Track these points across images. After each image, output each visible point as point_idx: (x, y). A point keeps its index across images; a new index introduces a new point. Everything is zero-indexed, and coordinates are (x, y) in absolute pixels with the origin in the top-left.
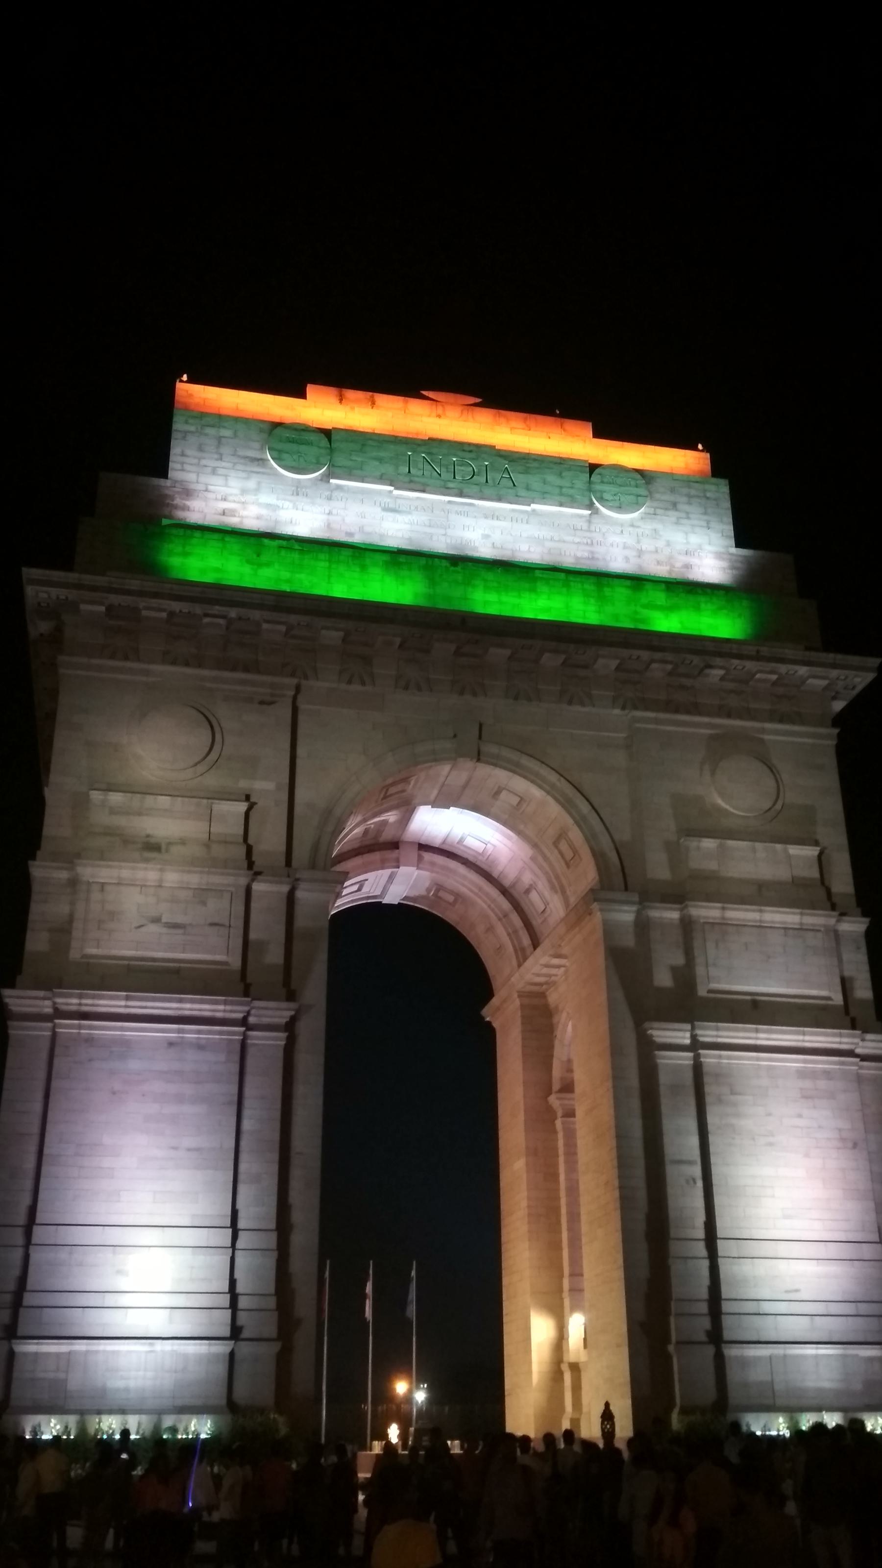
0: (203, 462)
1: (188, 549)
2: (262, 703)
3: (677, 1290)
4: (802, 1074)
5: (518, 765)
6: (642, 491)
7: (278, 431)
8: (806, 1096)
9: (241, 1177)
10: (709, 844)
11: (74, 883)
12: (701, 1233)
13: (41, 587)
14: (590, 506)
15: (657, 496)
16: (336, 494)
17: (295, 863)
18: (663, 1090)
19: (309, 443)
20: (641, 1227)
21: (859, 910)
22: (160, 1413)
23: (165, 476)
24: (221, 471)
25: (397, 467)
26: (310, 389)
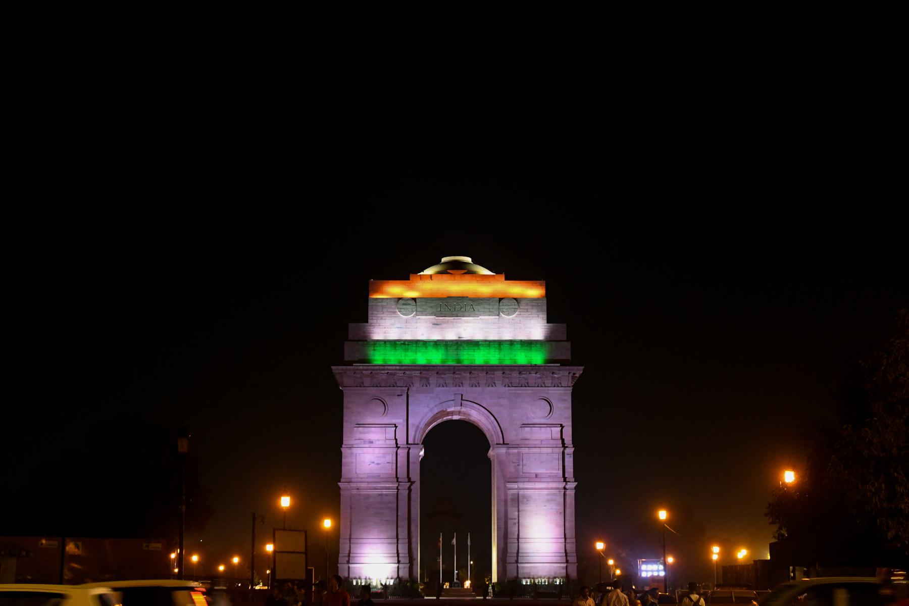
3: (509, 551)
4: (548, 495)
8: (548, 501)
10: (527, 429)
11: (352, 453)
14: (498, 315)
20: (502, 535)
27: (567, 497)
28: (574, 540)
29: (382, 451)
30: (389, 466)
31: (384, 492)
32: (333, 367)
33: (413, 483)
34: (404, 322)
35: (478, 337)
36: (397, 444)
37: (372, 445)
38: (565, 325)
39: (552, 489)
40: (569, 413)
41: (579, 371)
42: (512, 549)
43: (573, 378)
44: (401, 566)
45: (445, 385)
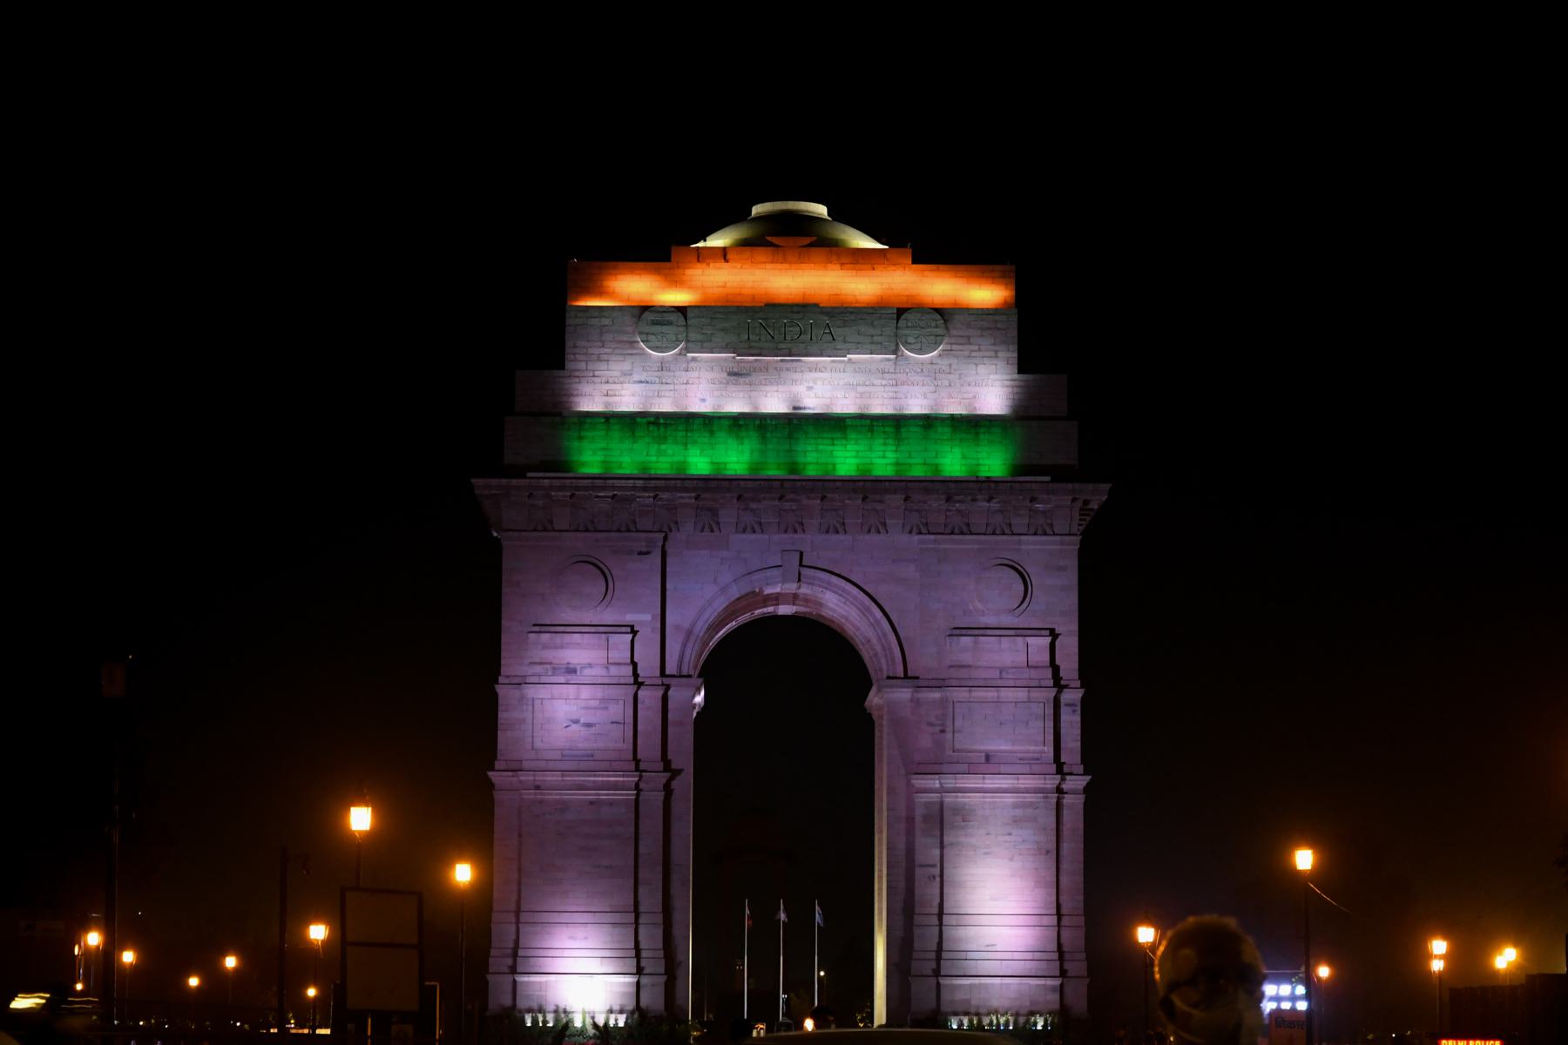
1: (584, 434)
2: (640, 553)
3: (917, 945)
4: (1016, 806)
5: (829, 583)
6: (940, 331)
7: (648, 316)
8: (1016, 821)
10: (966, 641)
11: (522, 698)
12: (936, 910)
14: (895, 352)
15: (954, 332)
16: (692, 364)
17: (668, 672)
18: (918, 819)
19: (669, 323)
21: (1078, 684)
23: (563, 367)
26: (674, 249)
29: (599, 692)
30: (617, 732)
31: (604, 795)
33: (680, 771)
34: (656, 372)
35: (845, 405)
36: (635, 675)
37: (573, 678)
39: (1027, 791)
40: (1072, 600)
41: (1098, 495)
42: (925, 940)
43: (1084, 511)
44: (645, 980)
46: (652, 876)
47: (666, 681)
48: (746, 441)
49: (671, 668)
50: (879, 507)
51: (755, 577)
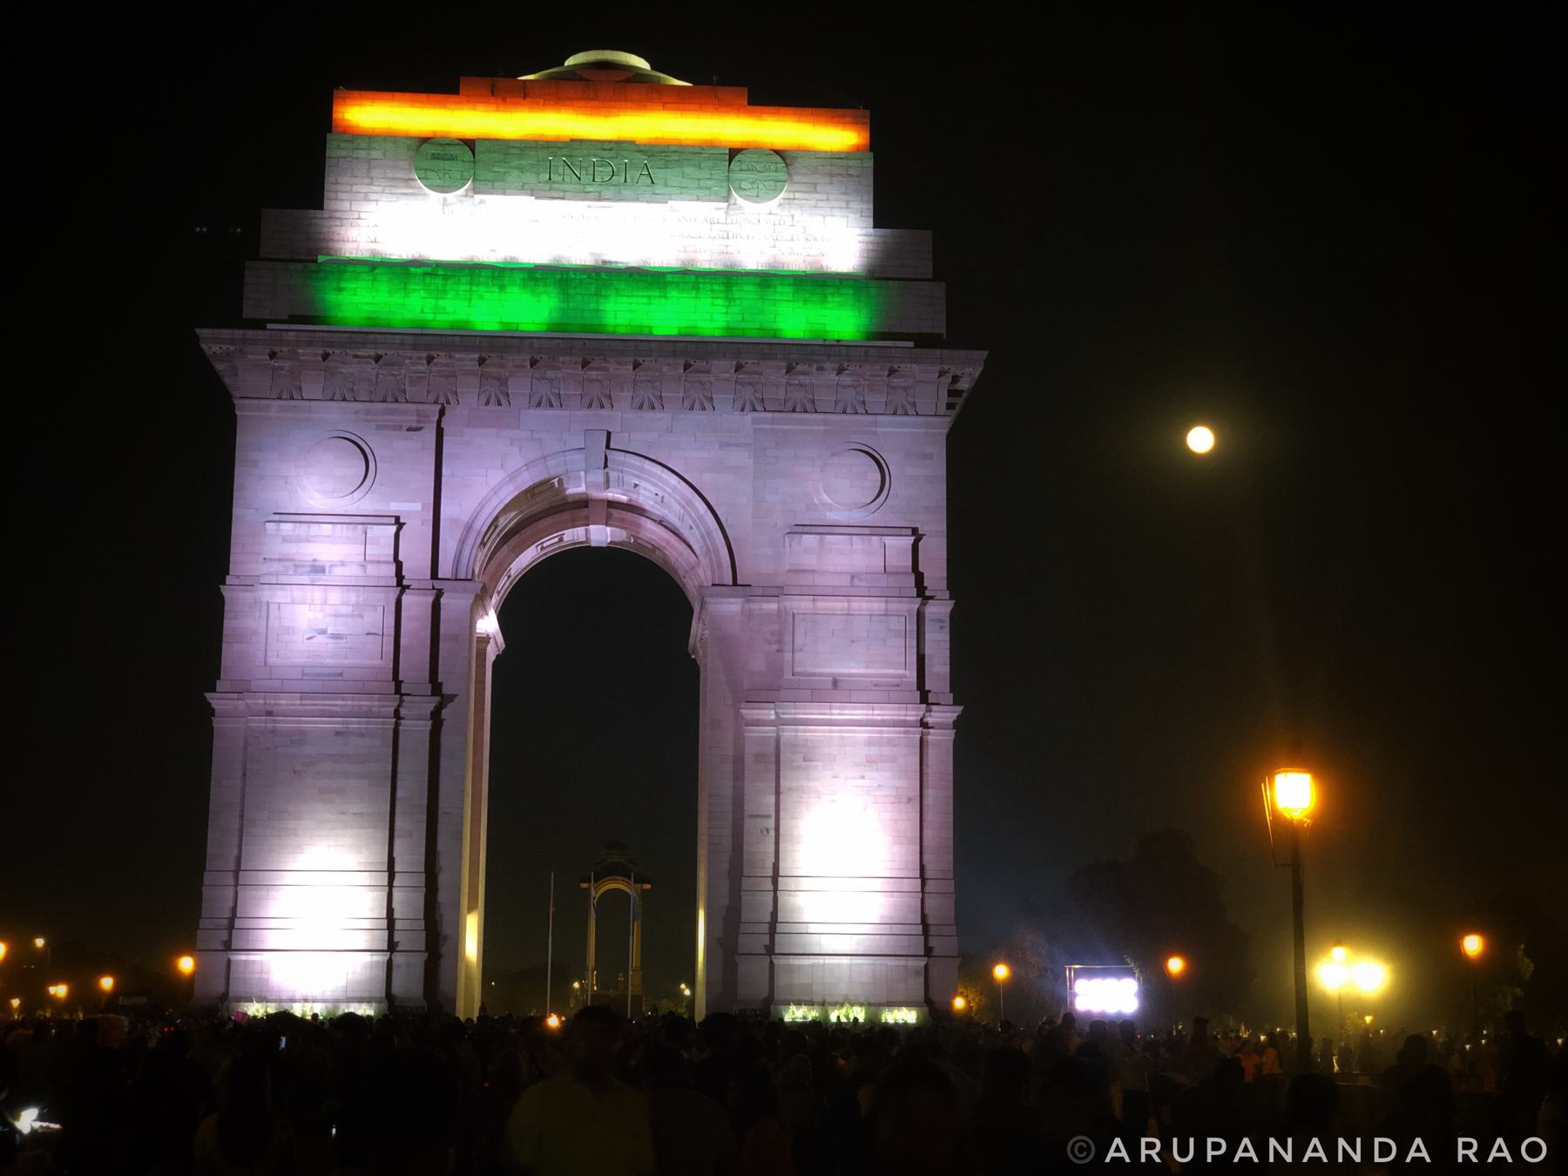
0: (355, 188)
1: (343, 285)
3: (744, 916)
4: (869, 743)
6: (782, 176)
8: (870, 761)
9: (396, 833)
10: (810, 540)
13: (214, 342)
14: (727, 198)
15: (796, 178)
18: (748, 760)
19: (453, 158)
22: (337, 1001)
24: (373, 196)
25: (538, 174)
27: (932, 754)
28: (950, 886)
29: (353, 597)
30: (373, 645)
32: (203, 332)
33: (452, 698)
35: (662, 257)
37: (320, 576)
38: (926, 236)
39: (883, 724)
40: (939, 493)
41: (969, 368)
43: (952, 393)
44: (398, 959)
45: (553, 401)
46: (411, 827)
47: (438, 584)
48: (544, 298)
49: (445, 570)
50: (704, 377)
51: (551, 462)
